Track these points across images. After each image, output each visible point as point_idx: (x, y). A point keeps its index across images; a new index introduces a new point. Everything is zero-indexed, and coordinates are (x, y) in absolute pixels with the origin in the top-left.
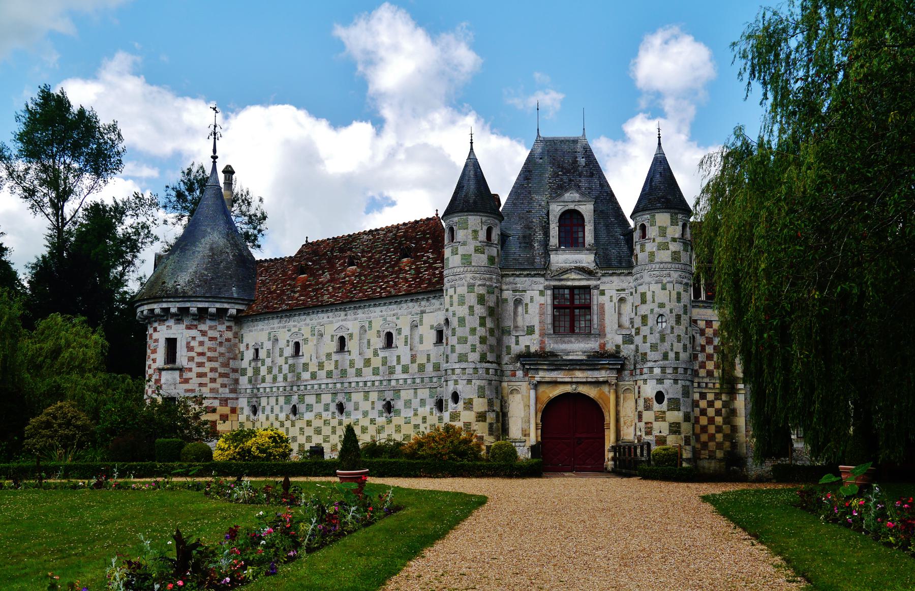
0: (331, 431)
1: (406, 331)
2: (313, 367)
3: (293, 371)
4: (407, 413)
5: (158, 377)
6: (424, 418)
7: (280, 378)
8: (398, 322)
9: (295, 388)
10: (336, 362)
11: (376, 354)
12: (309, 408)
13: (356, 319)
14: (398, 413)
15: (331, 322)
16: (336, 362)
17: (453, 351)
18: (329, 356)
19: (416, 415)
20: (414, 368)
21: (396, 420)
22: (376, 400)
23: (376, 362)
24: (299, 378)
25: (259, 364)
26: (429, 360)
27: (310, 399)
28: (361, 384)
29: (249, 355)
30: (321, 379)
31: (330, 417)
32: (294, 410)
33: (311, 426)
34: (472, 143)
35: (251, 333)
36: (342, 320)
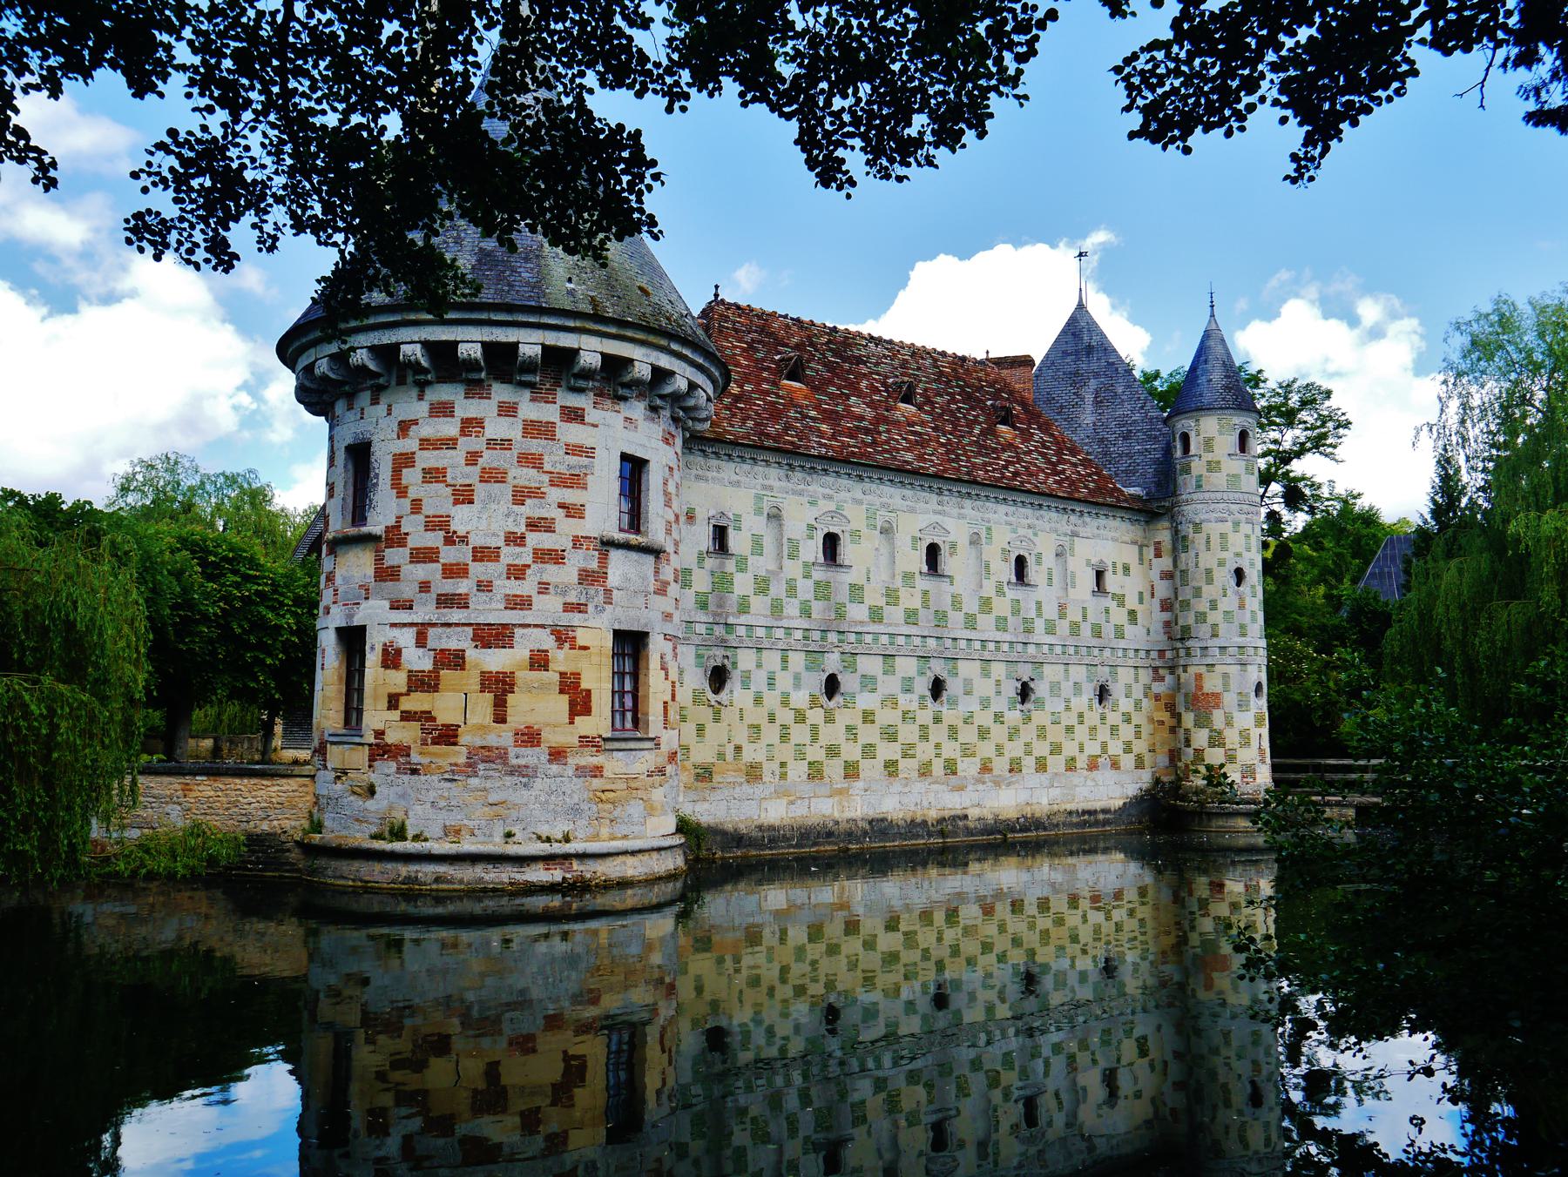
0: (917, 734)
1: (1049, 560)
2: (874, 597)
4: (1058, 706)
5: (594, 565)
6: (1081, 715)
7: (792, 609)
8: (1035, 539)
9: (833, 637)
10: (925, 593)
11: (1000, 592)
12: (868, 683)
13: (961, 517)
14: (1040, 704)
15: (912, 510)
16: (925, 593)
17: (1254, 620)
18: (908, 577)
19: (1068, 708)
20: (1063, 627)
21: (1039, 718)
22: (1003, 678)
23: (1002, 607)
24: (840, 615)
25: (730, 565)
26: (1085, 617)
27: (870, 665)
28: (977, 645)
29: (702, 537)
30: (897, 625)
31: (914, 706)
32: (832, 686)
33: (873, 722)
34: (1212, 306)
35: (702, 484)
36: (935, 512)
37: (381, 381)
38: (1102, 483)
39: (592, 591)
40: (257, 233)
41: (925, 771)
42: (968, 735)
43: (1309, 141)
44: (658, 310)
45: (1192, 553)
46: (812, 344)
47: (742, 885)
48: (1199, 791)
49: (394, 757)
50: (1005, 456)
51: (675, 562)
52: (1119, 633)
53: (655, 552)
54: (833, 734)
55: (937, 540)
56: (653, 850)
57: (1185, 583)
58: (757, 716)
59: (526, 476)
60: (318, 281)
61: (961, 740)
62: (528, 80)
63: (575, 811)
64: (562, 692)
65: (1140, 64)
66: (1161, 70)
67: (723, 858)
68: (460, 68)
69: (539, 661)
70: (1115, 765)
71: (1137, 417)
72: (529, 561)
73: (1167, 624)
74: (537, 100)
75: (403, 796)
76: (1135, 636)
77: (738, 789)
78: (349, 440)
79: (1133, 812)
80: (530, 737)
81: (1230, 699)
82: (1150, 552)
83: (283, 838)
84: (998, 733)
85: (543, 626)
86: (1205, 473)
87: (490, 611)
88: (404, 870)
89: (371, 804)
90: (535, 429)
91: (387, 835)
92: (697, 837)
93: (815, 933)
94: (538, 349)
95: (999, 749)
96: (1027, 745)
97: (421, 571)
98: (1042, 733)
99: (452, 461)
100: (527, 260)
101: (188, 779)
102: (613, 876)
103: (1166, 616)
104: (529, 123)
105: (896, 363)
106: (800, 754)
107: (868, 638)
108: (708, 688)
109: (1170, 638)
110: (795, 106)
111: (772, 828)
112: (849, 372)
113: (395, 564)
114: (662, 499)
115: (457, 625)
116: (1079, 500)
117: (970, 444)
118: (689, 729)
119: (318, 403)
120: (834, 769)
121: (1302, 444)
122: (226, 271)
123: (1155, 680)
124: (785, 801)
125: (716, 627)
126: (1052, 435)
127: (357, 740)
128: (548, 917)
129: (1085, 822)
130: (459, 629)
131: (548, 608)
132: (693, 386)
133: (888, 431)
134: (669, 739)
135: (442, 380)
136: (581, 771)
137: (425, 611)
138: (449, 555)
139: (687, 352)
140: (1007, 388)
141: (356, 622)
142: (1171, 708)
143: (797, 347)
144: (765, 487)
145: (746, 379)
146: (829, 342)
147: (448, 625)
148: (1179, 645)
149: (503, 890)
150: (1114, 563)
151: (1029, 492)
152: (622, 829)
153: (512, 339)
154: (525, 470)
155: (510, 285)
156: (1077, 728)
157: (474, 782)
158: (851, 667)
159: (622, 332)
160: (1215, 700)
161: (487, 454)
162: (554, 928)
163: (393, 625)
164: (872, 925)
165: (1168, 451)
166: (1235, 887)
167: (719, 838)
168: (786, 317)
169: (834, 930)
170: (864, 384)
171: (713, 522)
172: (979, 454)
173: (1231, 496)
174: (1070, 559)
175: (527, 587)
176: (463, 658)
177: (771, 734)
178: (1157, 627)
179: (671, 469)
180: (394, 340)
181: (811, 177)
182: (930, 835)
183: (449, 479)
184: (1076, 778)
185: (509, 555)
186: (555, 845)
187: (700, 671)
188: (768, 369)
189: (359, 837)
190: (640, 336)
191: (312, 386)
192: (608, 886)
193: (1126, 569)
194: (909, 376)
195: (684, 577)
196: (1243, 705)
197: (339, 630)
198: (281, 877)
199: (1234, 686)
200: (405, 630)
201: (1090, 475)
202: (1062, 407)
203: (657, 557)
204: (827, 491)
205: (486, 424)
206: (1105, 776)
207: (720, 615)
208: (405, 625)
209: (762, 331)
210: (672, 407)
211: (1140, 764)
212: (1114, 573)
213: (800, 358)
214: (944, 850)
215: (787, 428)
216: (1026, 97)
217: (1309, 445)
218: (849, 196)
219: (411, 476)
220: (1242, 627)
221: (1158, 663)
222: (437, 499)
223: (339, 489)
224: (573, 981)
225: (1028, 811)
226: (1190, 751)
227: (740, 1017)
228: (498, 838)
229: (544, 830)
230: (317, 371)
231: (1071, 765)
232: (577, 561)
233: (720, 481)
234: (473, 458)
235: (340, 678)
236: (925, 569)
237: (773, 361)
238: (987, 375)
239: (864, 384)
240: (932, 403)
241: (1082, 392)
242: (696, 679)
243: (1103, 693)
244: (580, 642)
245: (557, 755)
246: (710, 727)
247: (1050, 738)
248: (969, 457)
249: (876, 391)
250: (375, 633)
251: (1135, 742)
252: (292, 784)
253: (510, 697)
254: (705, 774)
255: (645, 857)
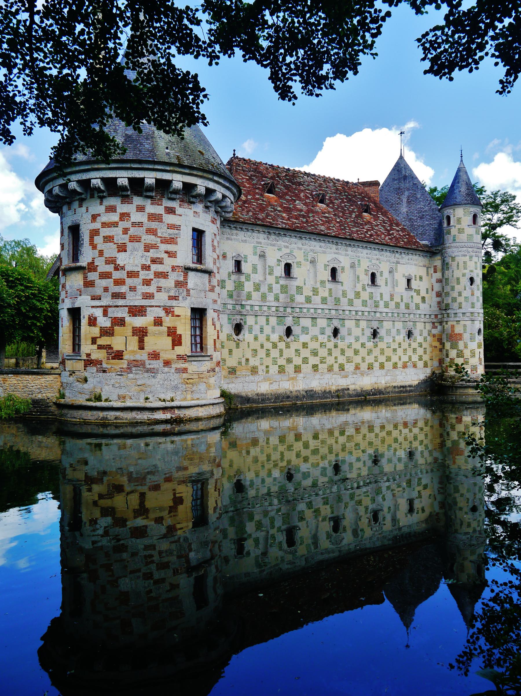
0: (327, 353)
1: (386, 274)
2: (307, 291)
3: (286, 292)
5: (181, 279)
6: (400, 344)
7: (271, 297)
8: (380, 265)
9: (289, 310)
11: (364, 289)
12: (305, 330)
13: (347, 255)
14: (382, 339)
15: (324, 252)
16: (330, 290)
17: (478, 301)
18: (323, 282)
19: (394, 341)
20: (392, 305)
21: (381, 345)
22: (365, 327)
23: (365, 296)
24: (292, 300)
25: (243, 278)
26: (402, 300)
27: (306, 322)
28: (354, 313)
29: (230, 266)
30: (318, 304)
31: (325, 340)
32: (289, 332)
33: (307, 347)
35: (230, 242)
36: (335, 253)
37: (83, 196)
38: (410, 239)
39: (181, 291)
40: (23, 126)
41: (330, 369)
42: (349, 353)
43: (508, 74)
44: (208, 162)
45: (451, 271)
46: (278, 177)
47: (250, 419)
48: (452, 377)
49: (95, 365)
50: (366, 227)
51: (218, 277)
52: (418, 307)
53: (209, 272)
54: (289, 353)
55: (335, 266)
56: (210, 404)
57: (447, 284)
58: (256, 345)
59: (150, 239)
60: (52, 149)
61: (346, 355)
62: (145, 51)
63: (176, 388)
64: (168, 335)
65: (429, 38)
66: (439, 40)
67: (241, 408)
68: (113, 46)
69: (158, 322)
70: (415, 366)
71: (426, 208)
72: (152, 276)
73: (439, 303)
74: (149, 60)
75: (100, 382)
76: (424, 308)
77: (247, 378)
78: (70, 224)
79: (423, 386)
80: (155, 356)
81: (466, 336)
82: (431, 270)
83: (48, 401)
84: (363, 352)
85: (159, 306)
86: (457, 234)
87: (136, 300)
88: (101, 414)
89: (86, 386)
90: (154, 217)
91: (93, 399)
92: (230, 399)
93: (282, 439)
94: (154, 181)
95: (363, 359)
96: (376, 357)
97: (104, 283)
98: (382, 352)
99: (117, 232)
100: (147, 139)
101: (5, 376)
102: (193, 416)
103: (439, 299)
104: (146, 71)
105: (317, 185)
106: (275, 362)
107: (305, 310)
108: (233, 333)
109: (440, 309)
110: (269, 61)
111: (262, 395)
112: (295, 189)
113: (92, 279)
114: (211, 248)
115: (121, 306)
116: (400, 247)
117: (350, 222)
118: (226, 351)
119: (54, 207)
120: (290, 369)
121: (502, 221)
122: (10, 144)
123: (433, 328)
124: (268, 383)
125: (236, 306)
126: (388, 217)
127: (79, 358)
128: (165, 434)
129: (401, 391)
130: (122, 308)
131: (161, 298)
132: (224, 197)
133: (313, 216)
134: (217, 356)
135: (110, 195)
136: (178, 370)
137: (106, 301)
138: (117, 275)
139: (221, 181)
140: (367, 195)
141: (76, 306)
142: (440, 340)
143: (272, 178)
144: (258, 243)
145: (248, 193)
146: (286, 175)
147: (117, 306)
148: (444, 312)
149: (145, 423)
150: (415, 276)
151: (377, 243)
152: (196, 396)
153: (142, 176)
154: (149, 236)
155: (140, 151)
156: (398, 349)
157: (131, 376)
158: (297, 323)
159: (192, 172)
160: (460, 336)
161: (132, 229)
162: (168, 439)
163: (93, 307)
164: (307, 436)
165: (440, 224)
166: (467, 419)
167: (239, 399)
168: (266, 164)
169: (291, 438)
170: (302, 195)
171: (234, 258)
172: (355, 226)
173: (469, 244)
174: (395, 274)
175: (152, 289)
176: (124, 321)
177: (262, 353)
178: (434, 304)
179: (215, 235)
180: (88, 177)
181: (276, 95)
182: (332, 397)
183: (115, 241)
184: (397, 372)
185: (143, 275)
186: (167, 403)
187: (230, 326)
188: (258, 188)
189: (81, 400)
190: (200, 173)
191: (52, 199)
192: (191, 420)
193: (421, 278)
194: (323, 190)
195: (222, 284)
196: (472, 339)
197: (69, 310)
198: (48, 418)
199: (468, 330)
200: (98, 309)
201: (405, 235)
202: (392, 204)
203: (210, 275)
204: (286, 244)
205: (131, 215)
206: (410, 370)
207: (238, 300)
208: (98, 307)
209: (256, 170)
210: (215, 206)
211: (426, 365)
212: (416, 280)
213: (273, 183)
214: (338, 404)
215: (268, 215)
216: (376, 54)
217: (505, 221)
218: (294, 104)
219: (98, 240)
220: (473, 304)
221: (434, 320)
222: (110, 250)
223: (66, 246)
224: (175, 462)
225: (376, 386)
226: (448, 359)
227: (249, 476)
228: (142, 400)
229: (162, 397)
230: (54, 193)
231: (395, 366)
232: (174, 277)
233: (237, 240)
234: (125, 231)
235: (70, 331)
236: (330, 279)
237: (261, 185)
238: (358, 190)
239: (302, 195)
240: (333, 203)
241: (401, 197)
242: (228, 329)
243: (410, 334)
244: (176, 313)
245: (167, 363)
246: (235, 350)
247: (386, 354)
248: (350, 228)
249: (308, 198)
250: (85, 310)
251: (424, 355)
252: (50, 378)
253: (146, 338)
254: (233, 371)
255: (207, 408)
